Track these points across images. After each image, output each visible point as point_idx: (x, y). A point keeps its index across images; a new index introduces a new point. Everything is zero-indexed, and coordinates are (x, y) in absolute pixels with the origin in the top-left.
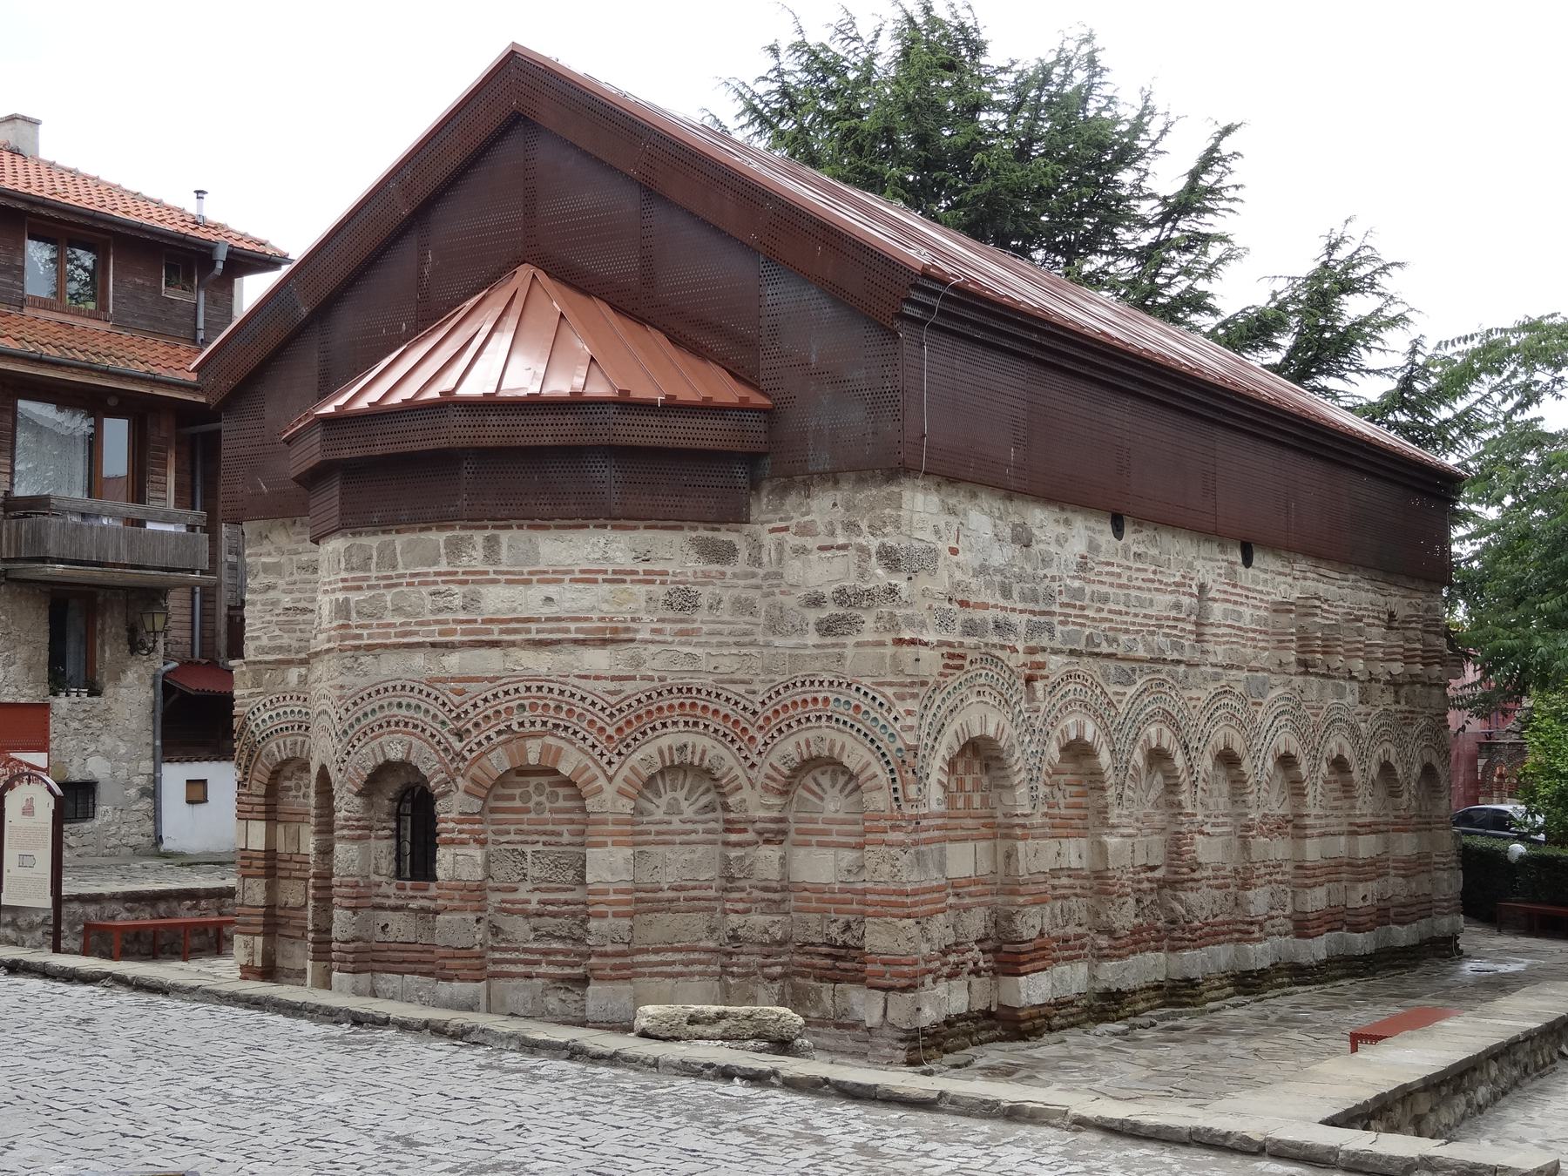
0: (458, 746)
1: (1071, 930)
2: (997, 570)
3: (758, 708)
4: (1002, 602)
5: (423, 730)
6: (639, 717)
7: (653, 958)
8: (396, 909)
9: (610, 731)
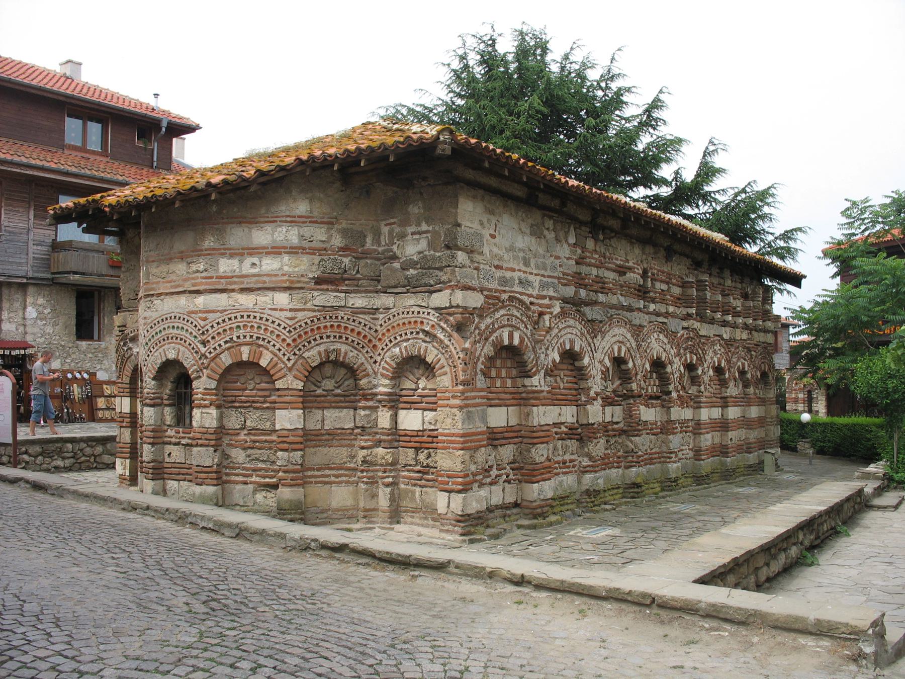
0: (203, 350)
1: (567, 457)
2: (520, 250)
3: (378, 328)
4: (524, 268)
6: (306, 333)
7: (316, 473)
8: (175, 444)
9: (289, 341)
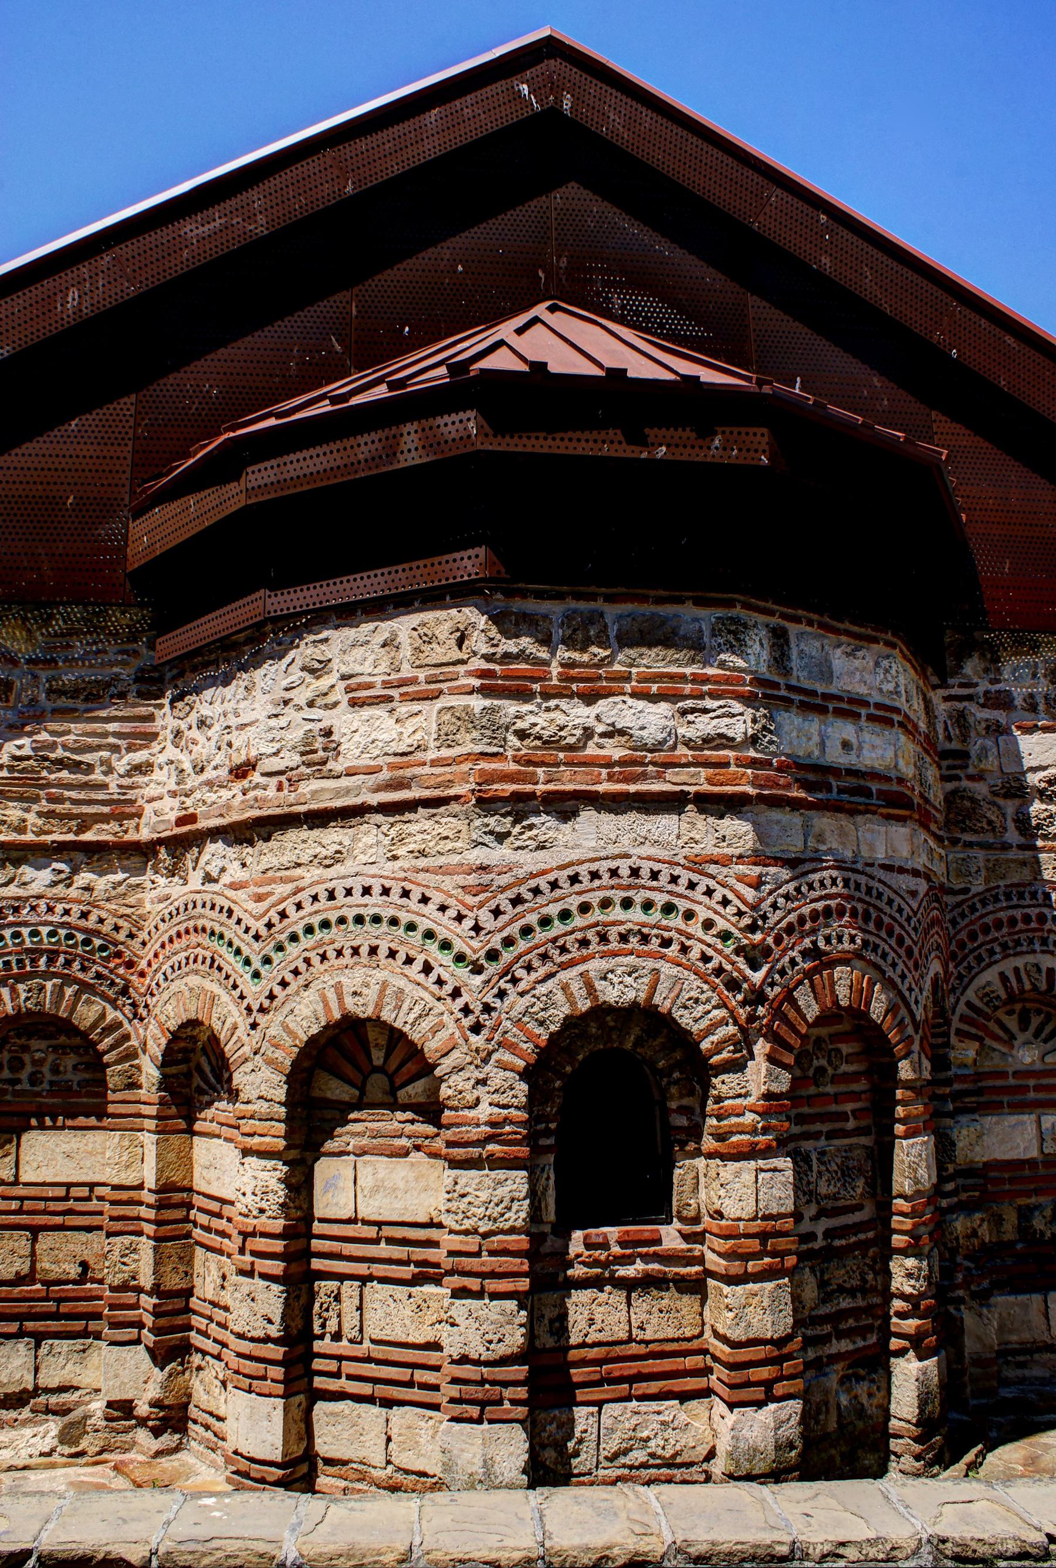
5: (684, 949)
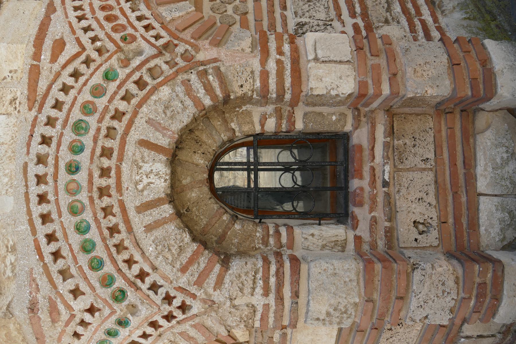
5: (118, 115)
